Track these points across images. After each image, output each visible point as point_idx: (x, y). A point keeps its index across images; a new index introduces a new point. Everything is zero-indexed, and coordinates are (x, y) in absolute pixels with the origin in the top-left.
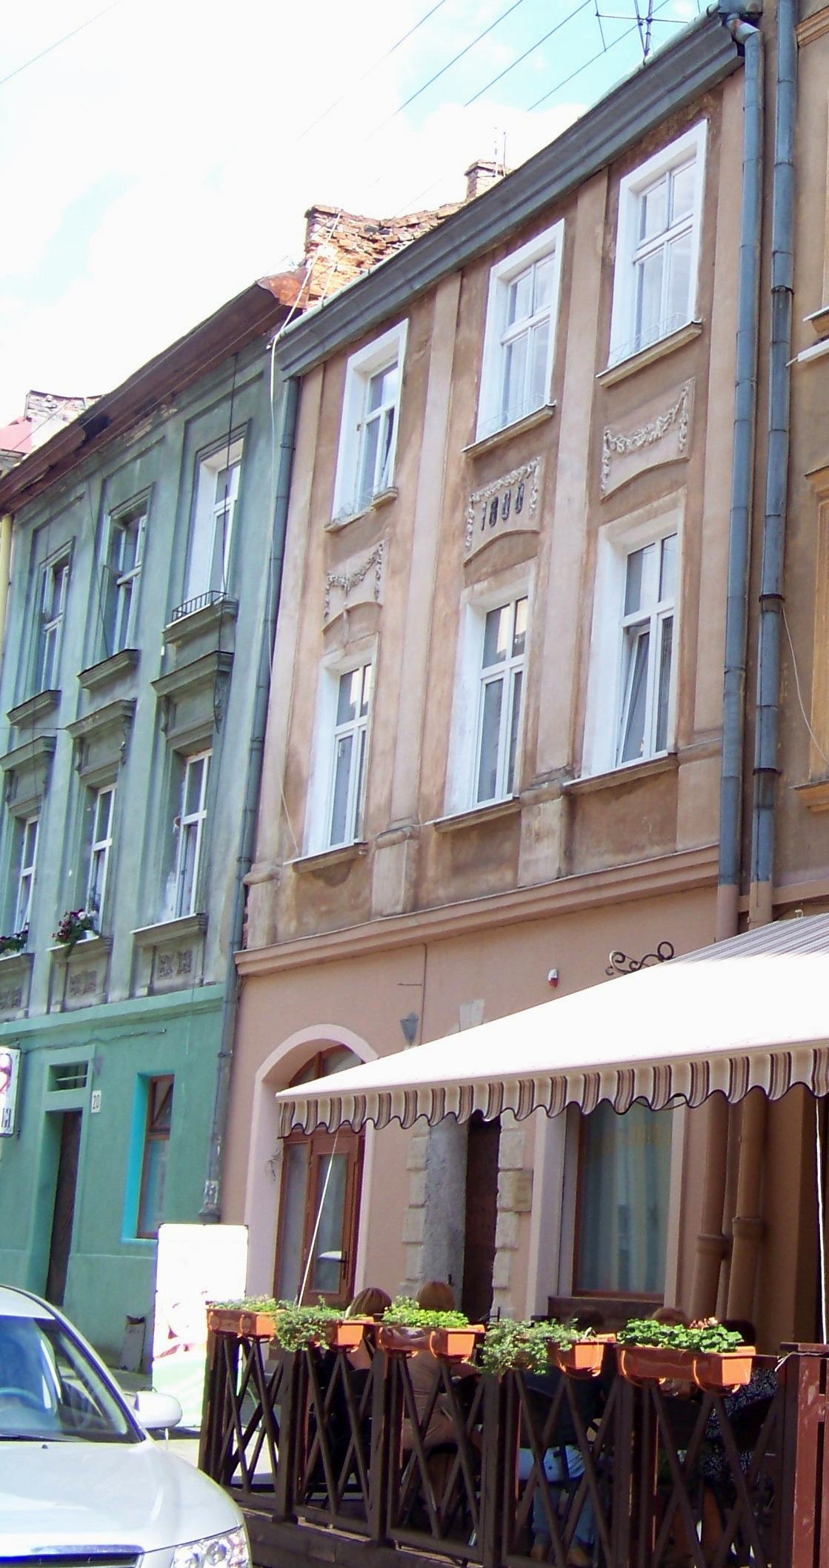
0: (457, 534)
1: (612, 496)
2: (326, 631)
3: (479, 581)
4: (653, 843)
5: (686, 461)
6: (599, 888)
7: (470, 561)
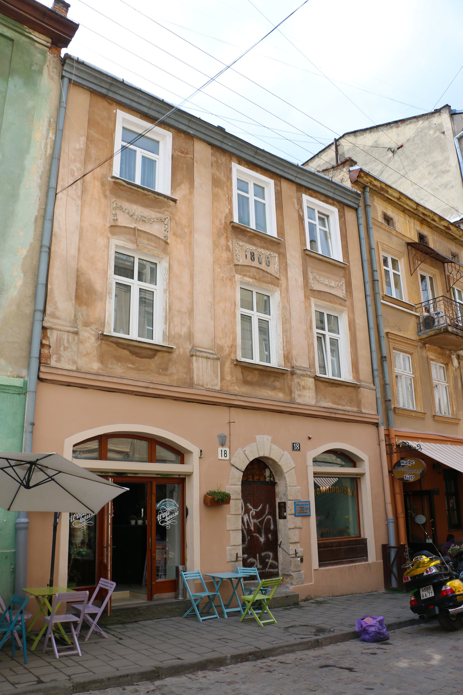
0: (224, 248)
1: (314, 290)
2: (112, 226)
3: (245, 275)
4: (348, 406)
5: (346, 301)
6: (335, 413)
7: (238, 265)
